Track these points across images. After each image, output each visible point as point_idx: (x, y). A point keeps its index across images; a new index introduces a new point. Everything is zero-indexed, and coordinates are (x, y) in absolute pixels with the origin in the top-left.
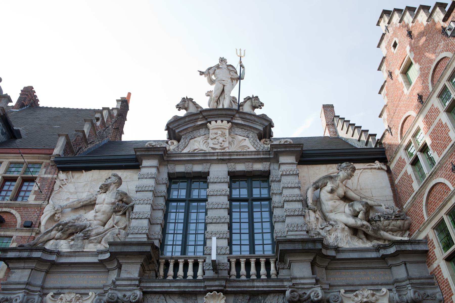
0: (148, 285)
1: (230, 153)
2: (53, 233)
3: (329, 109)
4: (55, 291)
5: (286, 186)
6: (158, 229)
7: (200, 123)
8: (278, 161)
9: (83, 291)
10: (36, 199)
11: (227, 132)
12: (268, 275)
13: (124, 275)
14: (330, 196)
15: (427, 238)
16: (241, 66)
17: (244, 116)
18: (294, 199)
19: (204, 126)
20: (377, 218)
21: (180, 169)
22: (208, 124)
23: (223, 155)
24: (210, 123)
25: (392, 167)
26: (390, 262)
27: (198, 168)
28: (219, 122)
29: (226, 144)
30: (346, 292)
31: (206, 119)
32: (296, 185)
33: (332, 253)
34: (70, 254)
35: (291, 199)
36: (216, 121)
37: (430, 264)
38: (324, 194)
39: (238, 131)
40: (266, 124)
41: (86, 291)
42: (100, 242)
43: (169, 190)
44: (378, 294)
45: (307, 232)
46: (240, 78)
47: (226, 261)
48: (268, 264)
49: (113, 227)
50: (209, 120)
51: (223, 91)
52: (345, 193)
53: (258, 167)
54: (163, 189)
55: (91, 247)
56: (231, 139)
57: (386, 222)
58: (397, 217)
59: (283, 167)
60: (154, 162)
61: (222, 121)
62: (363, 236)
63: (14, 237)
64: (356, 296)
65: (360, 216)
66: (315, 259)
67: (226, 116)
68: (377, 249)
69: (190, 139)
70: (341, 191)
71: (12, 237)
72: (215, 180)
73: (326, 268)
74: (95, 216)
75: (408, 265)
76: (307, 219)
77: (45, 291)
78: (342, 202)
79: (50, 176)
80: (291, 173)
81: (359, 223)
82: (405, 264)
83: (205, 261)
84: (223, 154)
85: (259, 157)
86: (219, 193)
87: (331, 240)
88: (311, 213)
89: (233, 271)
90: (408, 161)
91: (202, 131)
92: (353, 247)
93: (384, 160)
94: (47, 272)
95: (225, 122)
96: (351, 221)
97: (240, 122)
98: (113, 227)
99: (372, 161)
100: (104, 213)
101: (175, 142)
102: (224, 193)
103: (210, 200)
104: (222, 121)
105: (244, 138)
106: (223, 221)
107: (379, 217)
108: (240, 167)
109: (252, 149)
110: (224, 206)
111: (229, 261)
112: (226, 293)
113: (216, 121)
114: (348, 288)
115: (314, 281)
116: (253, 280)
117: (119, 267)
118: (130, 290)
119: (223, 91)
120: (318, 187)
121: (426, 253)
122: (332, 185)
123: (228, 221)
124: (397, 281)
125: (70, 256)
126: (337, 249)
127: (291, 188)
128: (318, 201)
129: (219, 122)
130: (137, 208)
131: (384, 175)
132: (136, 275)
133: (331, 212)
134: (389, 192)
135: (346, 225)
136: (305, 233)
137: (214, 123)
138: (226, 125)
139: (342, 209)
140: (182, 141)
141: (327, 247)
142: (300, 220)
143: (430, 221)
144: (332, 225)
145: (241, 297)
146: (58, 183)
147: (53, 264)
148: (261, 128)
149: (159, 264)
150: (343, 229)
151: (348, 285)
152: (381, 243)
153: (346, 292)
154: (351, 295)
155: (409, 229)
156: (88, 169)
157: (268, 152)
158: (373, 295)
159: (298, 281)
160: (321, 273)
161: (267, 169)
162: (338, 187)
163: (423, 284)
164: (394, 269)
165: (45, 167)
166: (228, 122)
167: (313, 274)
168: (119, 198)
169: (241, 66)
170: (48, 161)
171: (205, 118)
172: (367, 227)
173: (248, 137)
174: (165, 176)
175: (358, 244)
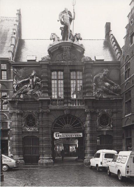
16: (74, 12)
46: (74, 19)
69: (57, 55)
167: (92, 105)
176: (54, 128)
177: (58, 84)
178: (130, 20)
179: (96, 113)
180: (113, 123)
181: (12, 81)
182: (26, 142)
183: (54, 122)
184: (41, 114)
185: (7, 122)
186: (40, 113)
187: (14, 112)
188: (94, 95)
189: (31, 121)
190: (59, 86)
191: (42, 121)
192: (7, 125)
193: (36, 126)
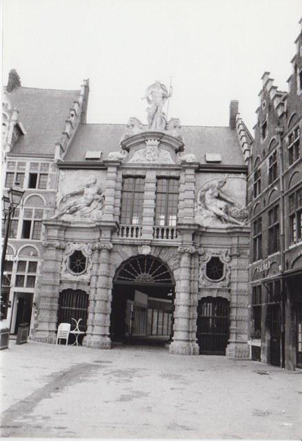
6: (118, 209)
7: (141, 140)
8: (185, 171)
10: (51, 188)
13: (103, 236)
16: (171, 87)
19: (144, 142)
21: (129, 173)
26: (232, 235)
27: (139, 173)
29: (156, 157)
33: (204, 230)
43: (123, 184)
53: (173, 174)
54: (119, 185)
67: (157, 136)
70: (216, 194)
73: (201, 236)
75: (240, 238)
82: (238, 237)
84: (153, 165)
91: (142, 145)
94: (65, 231)
99: (240, 173)
101: (126, 152)
103: (145, 193)
109: (172, 162)
111: (154, 229)
112: (151, 246)
117: (101, 231)
130: (107, 199)
138: (157, 143)
146: (61, 178)
147: (68, 227)
150: (213, 217)
157: (180, 166)
160: (197, 239)
164: (233, 238)
167: (193, 239)
170: (52, 163)
171: (144, 137)
174: (121, 177)
175: (219, 225)
176: (119, 279)
178: (262, 101)
179: (200, 255)
180: (230, 274)
181: (54, 192)
183: (119, 268)
184: (97, 251)
185: (36, 263)
186: (95, 250)
192: (36, 266)
193: (86, 271)
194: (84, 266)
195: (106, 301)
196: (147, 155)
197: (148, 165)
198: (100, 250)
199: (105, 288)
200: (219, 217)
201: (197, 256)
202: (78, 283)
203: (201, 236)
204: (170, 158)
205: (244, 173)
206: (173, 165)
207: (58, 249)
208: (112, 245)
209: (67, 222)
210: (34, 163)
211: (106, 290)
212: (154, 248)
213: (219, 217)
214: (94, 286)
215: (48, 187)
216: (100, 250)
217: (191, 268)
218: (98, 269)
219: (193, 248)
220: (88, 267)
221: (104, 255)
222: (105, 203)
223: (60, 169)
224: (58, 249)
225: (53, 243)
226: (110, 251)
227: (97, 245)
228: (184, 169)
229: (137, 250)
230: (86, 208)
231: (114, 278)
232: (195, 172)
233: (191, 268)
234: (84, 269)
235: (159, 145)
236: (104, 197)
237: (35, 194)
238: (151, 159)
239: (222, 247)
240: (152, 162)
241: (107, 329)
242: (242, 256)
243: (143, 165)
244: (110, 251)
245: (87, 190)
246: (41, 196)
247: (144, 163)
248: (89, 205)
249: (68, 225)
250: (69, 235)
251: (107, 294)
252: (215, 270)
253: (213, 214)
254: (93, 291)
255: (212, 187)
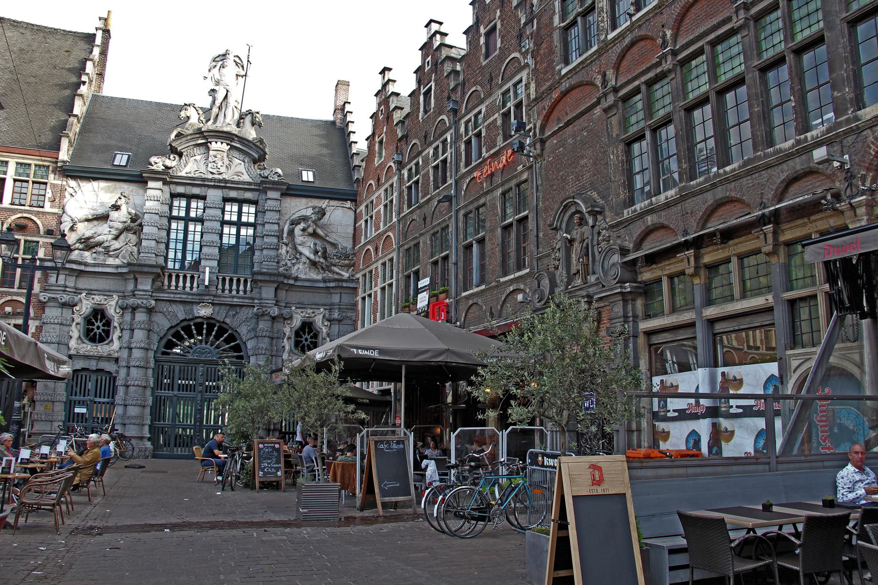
0: (158, 295)
1: (225, 181)
2: (77, 245)
3: (344, 87)
4: (86, 292)
5: (268, 221)
6: (163, 246)
8: (266, 193)
9: (107, 293)
10: (51, 207)
11: (225, 154)
12: (245, 292)
13: (140, 287)
14: (301, 233)
15: (358, 279)
16: (248, 61)
17: (242, 140)
18: (273, 234)
20: (332, 256)
21: (180, 189)
22: (209, 144)
23: (219, 182)
24: (210, 143)
25: (358, 211)
26: (332, 291)
27: (196, 191)
28: (219, 143)
29: (223, 170)
30: (296, 308)
31: (207, 139)
32: (276, 221)
33: (291, 282)
34: (94, 265)
35: (270, 234)
36: (216, 142)
37: (356, 297)
38: (298, 230)
39: (235, 153)
40: (262, 153)
41: (111, 293)
42: (117, 257)
44: (317, 311)
45: (278, 263)
47: (215, 278)
48: (246, 281)
49: (127, 244)
50: (209, 140)
51: (227, 95)
52: (314, 231)
53: (248, 195)
55: (111, 261)
56: (228, 162)
57: (337, 261)
58: (347, 257)
59: (270, 202)
60: (159, 184)
61: (222, 143)
62: (319, 267)
63: (41, 243)
64: (302, 312)
65: (319, 254)
66: (278, 286)
68: (324, 281)
70: (310, 230)
71: (38, 242)
72: (211, 206)
73: (287, 290)
74: (110, 231)
76: (280, 251)
77: (78, 291)
78: (310, 238)
79: (59, 182)
80: (275, 209)
81: (317, 259)
83: (199, 277)
84: (220, 181)
85: (250, 187)
86: (214, 218)
87: (294, 271)
88: (284, 247)
89: (220, 286)
90: (364, 219)
92: (308, 277)
93: (354, 201)
95: (225, 144)
96: (312, 257)
97: (238, 146)
98: (127, 244)
99: (346, 200)
100: (117, 229)
101: (177, 158)
102: (217, 219)
104: (222, 143)
105: (241, 162)
106: (215, 244)
107: (334, 255)
108: (233, 194)
109: (246, 178)
110: (217, 232)
112: (213, 304)
113: (216, 142)
114: (298, 306)
115: (275, 302)
116: (233, 297)
117: (136, 279)
118: (146, 299)
119: (227, 95)
120: (295, 223)
121: (355, 289)
122: (304, 225)
123: (219, 245)
124: (332, 304)
125: (95, 266)
126: (296, 279)
127: (272, 223)
128: (291, 233)
129: (219, 143)
130: (146, 229)
131: (351, 214)
132: (148, 287)
133: (300, 245)
134: (351, 230)
135: (308, 258)
136: (275, 264)
137: (213, 143)
138: (225, 147)
139: (308, 244)
140: (184, 158)
141: (288, 277)
142: (273, 253)
143: (362, 270)
144: (297, 259)
145: (224, 307)
148: (256, 156)
149: (164, 274)
150: (305, 263)
151: (299, 303)
152: (330, 275)
153: (296, 308)
154: (299, 311)
155: (353, 265)
156: (95, 179)
157: (259, 185)
158: (313, 313)
159: (264, 301)
160: (282, 294)
161: (256, 199)
162: (309, 226)
163: (347, 309)
165: (53, 171)
166: (228, 144)
167: (275, 296)
168: (130, 217)
169: (248, 61)
171: (205, 137)
172: (322, 263)
173: (244, 162)
174: (168, 196)
175: (314, 275)
176: (164, 353)
177: (186, 231)
179: (285, 319)
182: (77, 386)
183: (165, 335)
187: (53, 298)
188: (281, 269)
189: (98, 328)
190: (190, 237)
191: (130, 329)
194: (107, 333)
195: (145, 387)
196: (210, 165)
197: (211, 180)
198: (134, 309)
199: (141, 367)
200: (314, 264)
201: (282, 320)
202: (100, 358)
203: (287, 290)
204: (244, 171)
205: (352, 201)
206: (249, 184)
207: (64, 305)
208: (153, 302)
209: (80, 263)
210: (21, 164)
211: (144, 369)
212: (217, 308)
213: (314, 264)
214: (124, 364)
215: (47, 205)
216: (134, 309)
217: (272, 338)
218: (132, 337)
219: (276, 309)
220: (116, 335)
221: (140, 316)
222: (143, 236)
223: (67, 176)
224: (64, 305)
225: (58, 296)
226: (150, 311)
227: (131, 301)
228: (264, 191)
229: (192, 310)
230: (114, 242)
231: (155, 352)
232: (283, 195)
233: (272, 338)
234: (108, 336)
235: (229, 149)
236: (141, 225)
237: (25, 215)
238: (214, 171)
239: (317, 305)
240: (217, 176)
241: (147, 428)
242: (345, 322)
243: (204, 180)
244: (150, 311)
245: (114, 215)
246: (35, 219)
247: (204, 176)
248: (116, 238)
249: (82, 268)
250: (84, 283)
251: (146, 375)
252: (306, 340)
253: (304, 259)
254: (123, 372)
255: (304, 219)
